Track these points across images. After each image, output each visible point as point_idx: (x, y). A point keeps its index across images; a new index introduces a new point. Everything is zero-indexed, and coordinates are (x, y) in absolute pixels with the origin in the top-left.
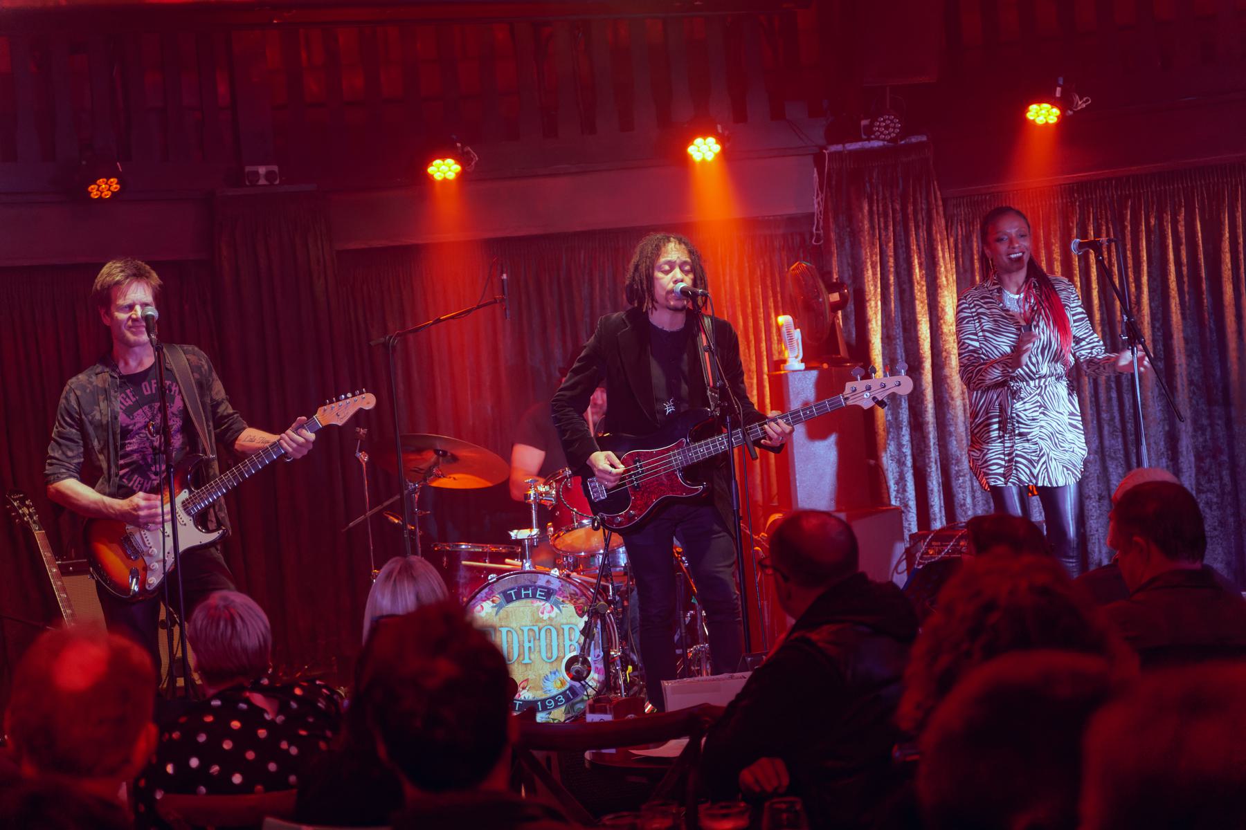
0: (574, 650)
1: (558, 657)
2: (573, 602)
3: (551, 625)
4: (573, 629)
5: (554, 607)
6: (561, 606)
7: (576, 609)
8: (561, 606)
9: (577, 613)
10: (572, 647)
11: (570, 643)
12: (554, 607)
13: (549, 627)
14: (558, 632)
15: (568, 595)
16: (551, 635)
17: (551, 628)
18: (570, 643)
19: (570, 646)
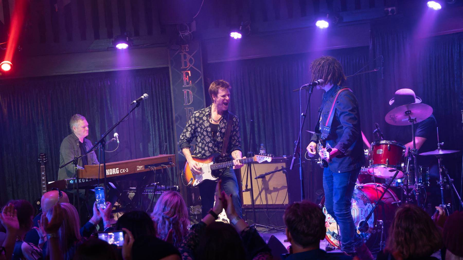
0: (363, 219)
1: (357, 221)
2: (362, 199)
3: (355, 208)
4: (362, 210)
5: (356, 201)
6: (358, 200)
7: (364, 202)
8: (358, 200)
9: (364, 203)
10: (362, 217)
11: (361, 216)
12: (356, 201)
13: (355, 209)
14: (357, 211)
15: (361, 196)
16: (354, 212)
17: (355, 209)
18: (361, 216)
19: (361, 217)
